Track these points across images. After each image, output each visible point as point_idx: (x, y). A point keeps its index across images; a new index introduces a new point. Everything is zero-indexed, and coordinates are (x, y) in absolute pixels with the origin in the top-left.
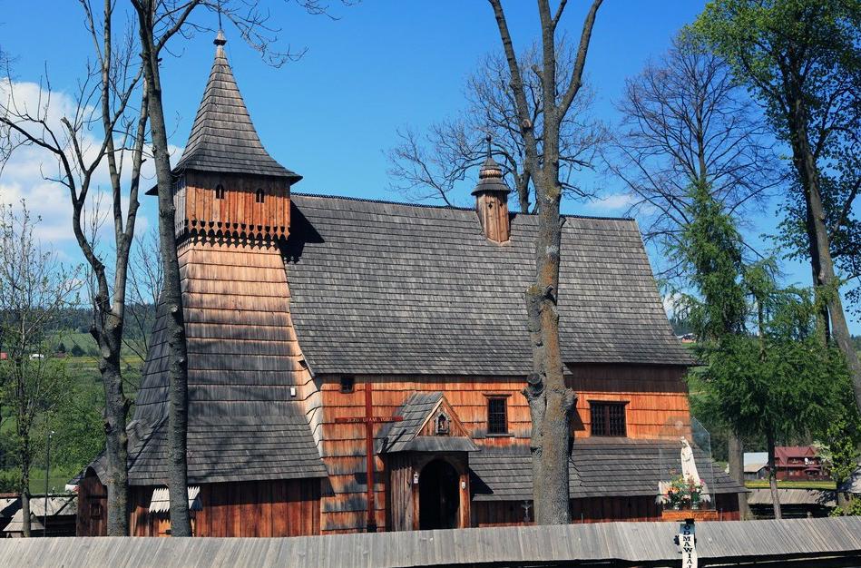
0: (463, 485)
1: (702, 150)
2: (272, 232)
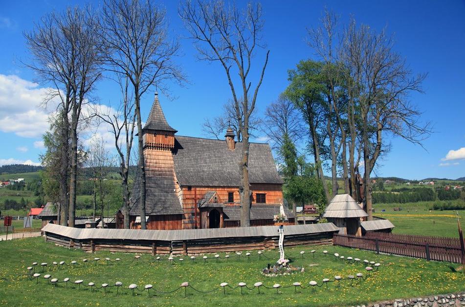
0: (221, 216)
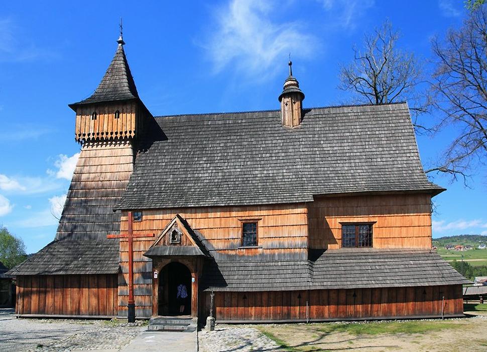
0: (193, 280)
2: (124, 135)
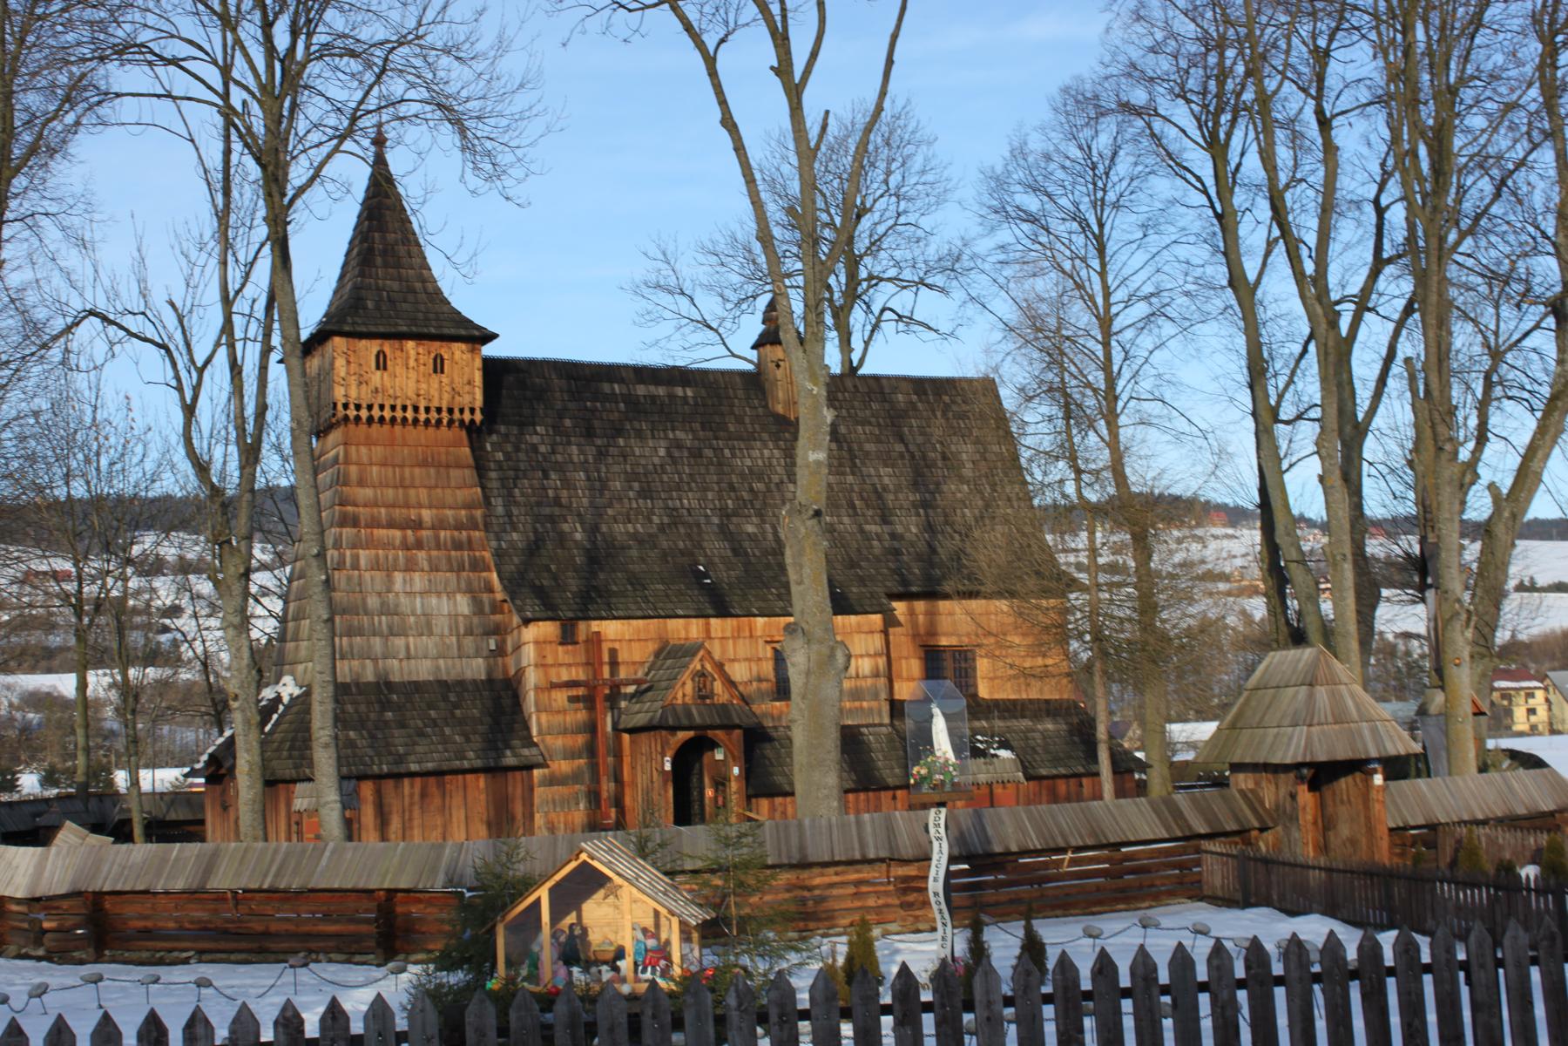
1: (1103, 265)
2: (457, 415)
